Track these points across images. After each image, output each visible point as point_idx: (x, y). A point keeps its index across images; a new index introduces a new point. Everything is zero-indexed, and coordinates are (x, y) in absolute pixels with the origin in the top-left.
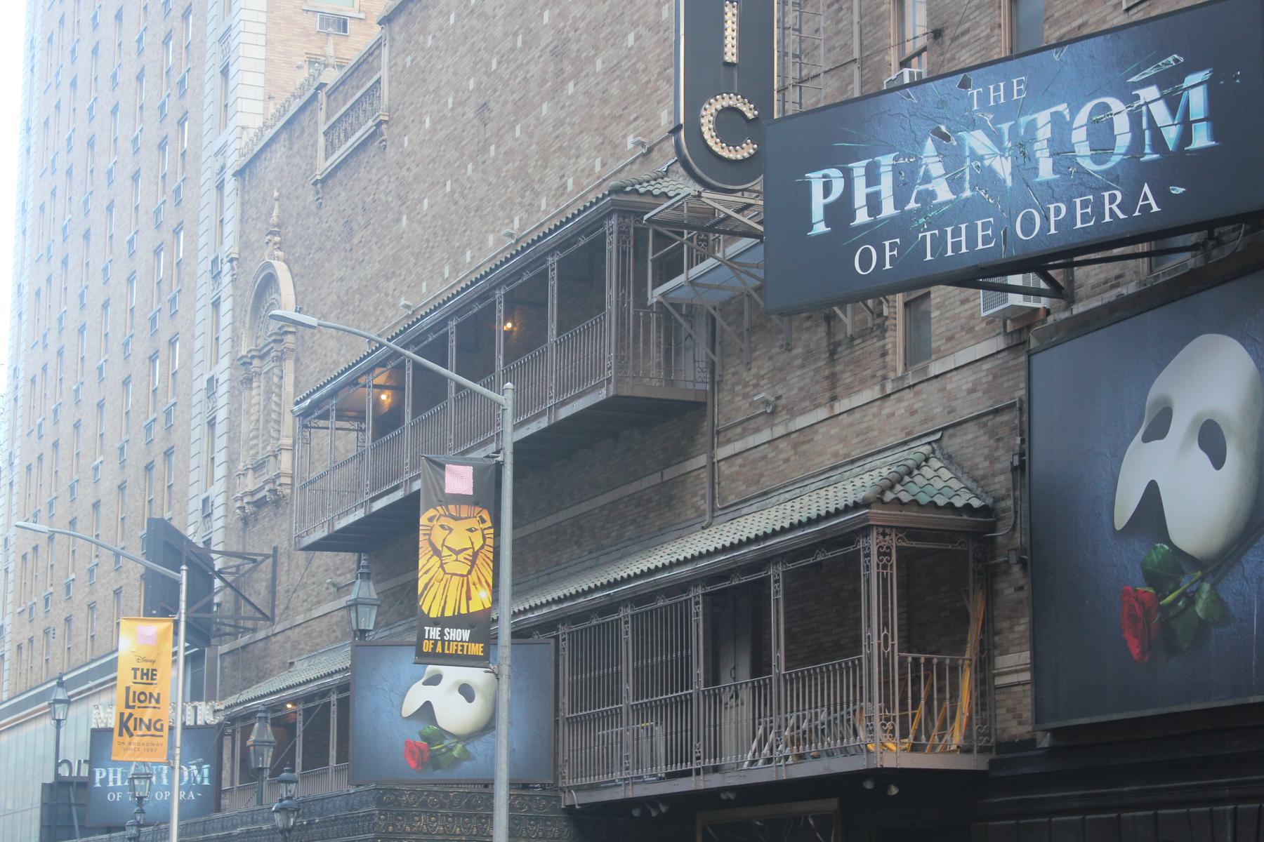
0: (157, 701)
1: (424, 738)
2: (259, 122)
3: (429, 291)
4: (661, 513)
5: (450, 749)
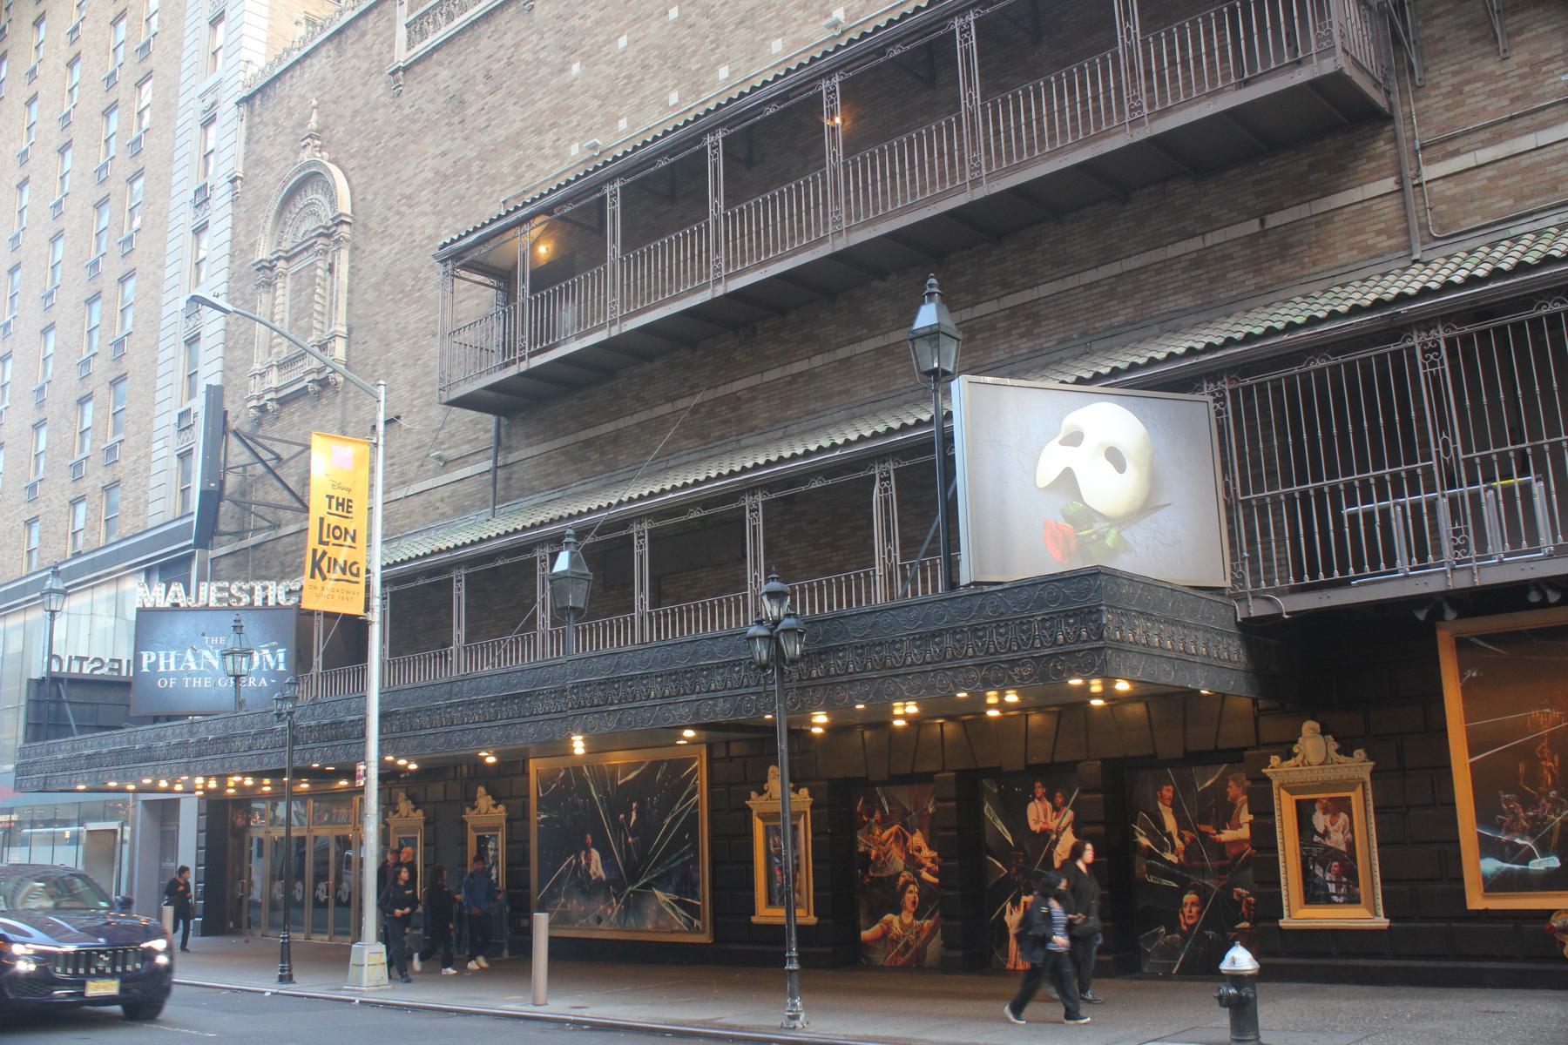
0: (353, 539)
1: (1069, 519)
2: (261, 62)
3: (632, 126)
4: (1276, 259)
5: (1102, 536)
